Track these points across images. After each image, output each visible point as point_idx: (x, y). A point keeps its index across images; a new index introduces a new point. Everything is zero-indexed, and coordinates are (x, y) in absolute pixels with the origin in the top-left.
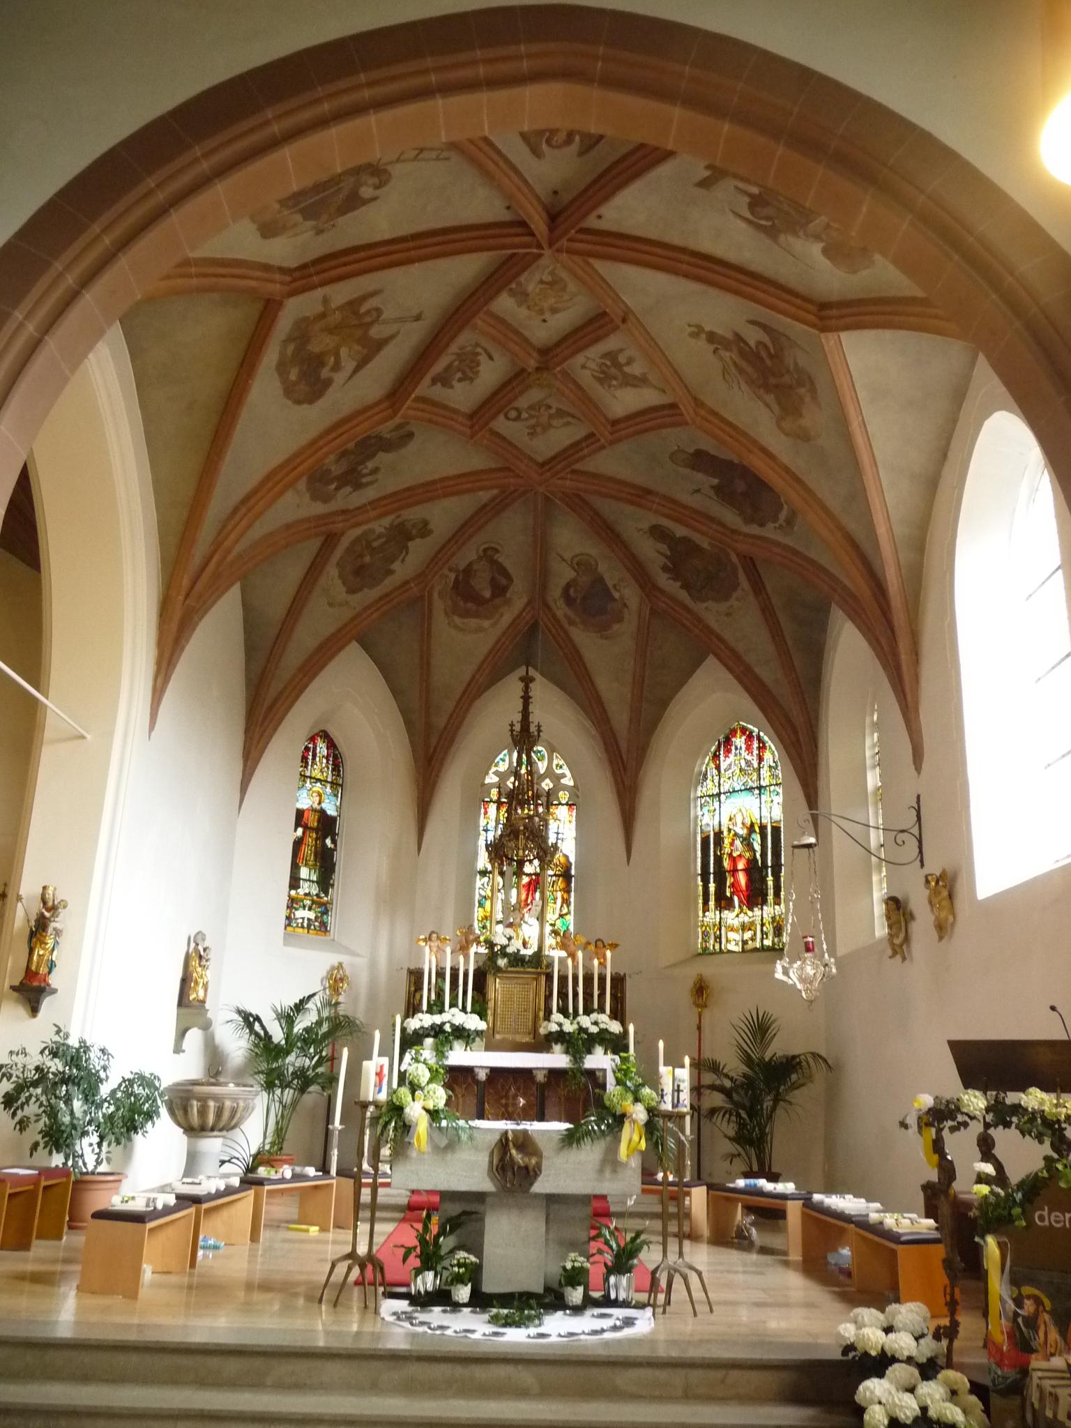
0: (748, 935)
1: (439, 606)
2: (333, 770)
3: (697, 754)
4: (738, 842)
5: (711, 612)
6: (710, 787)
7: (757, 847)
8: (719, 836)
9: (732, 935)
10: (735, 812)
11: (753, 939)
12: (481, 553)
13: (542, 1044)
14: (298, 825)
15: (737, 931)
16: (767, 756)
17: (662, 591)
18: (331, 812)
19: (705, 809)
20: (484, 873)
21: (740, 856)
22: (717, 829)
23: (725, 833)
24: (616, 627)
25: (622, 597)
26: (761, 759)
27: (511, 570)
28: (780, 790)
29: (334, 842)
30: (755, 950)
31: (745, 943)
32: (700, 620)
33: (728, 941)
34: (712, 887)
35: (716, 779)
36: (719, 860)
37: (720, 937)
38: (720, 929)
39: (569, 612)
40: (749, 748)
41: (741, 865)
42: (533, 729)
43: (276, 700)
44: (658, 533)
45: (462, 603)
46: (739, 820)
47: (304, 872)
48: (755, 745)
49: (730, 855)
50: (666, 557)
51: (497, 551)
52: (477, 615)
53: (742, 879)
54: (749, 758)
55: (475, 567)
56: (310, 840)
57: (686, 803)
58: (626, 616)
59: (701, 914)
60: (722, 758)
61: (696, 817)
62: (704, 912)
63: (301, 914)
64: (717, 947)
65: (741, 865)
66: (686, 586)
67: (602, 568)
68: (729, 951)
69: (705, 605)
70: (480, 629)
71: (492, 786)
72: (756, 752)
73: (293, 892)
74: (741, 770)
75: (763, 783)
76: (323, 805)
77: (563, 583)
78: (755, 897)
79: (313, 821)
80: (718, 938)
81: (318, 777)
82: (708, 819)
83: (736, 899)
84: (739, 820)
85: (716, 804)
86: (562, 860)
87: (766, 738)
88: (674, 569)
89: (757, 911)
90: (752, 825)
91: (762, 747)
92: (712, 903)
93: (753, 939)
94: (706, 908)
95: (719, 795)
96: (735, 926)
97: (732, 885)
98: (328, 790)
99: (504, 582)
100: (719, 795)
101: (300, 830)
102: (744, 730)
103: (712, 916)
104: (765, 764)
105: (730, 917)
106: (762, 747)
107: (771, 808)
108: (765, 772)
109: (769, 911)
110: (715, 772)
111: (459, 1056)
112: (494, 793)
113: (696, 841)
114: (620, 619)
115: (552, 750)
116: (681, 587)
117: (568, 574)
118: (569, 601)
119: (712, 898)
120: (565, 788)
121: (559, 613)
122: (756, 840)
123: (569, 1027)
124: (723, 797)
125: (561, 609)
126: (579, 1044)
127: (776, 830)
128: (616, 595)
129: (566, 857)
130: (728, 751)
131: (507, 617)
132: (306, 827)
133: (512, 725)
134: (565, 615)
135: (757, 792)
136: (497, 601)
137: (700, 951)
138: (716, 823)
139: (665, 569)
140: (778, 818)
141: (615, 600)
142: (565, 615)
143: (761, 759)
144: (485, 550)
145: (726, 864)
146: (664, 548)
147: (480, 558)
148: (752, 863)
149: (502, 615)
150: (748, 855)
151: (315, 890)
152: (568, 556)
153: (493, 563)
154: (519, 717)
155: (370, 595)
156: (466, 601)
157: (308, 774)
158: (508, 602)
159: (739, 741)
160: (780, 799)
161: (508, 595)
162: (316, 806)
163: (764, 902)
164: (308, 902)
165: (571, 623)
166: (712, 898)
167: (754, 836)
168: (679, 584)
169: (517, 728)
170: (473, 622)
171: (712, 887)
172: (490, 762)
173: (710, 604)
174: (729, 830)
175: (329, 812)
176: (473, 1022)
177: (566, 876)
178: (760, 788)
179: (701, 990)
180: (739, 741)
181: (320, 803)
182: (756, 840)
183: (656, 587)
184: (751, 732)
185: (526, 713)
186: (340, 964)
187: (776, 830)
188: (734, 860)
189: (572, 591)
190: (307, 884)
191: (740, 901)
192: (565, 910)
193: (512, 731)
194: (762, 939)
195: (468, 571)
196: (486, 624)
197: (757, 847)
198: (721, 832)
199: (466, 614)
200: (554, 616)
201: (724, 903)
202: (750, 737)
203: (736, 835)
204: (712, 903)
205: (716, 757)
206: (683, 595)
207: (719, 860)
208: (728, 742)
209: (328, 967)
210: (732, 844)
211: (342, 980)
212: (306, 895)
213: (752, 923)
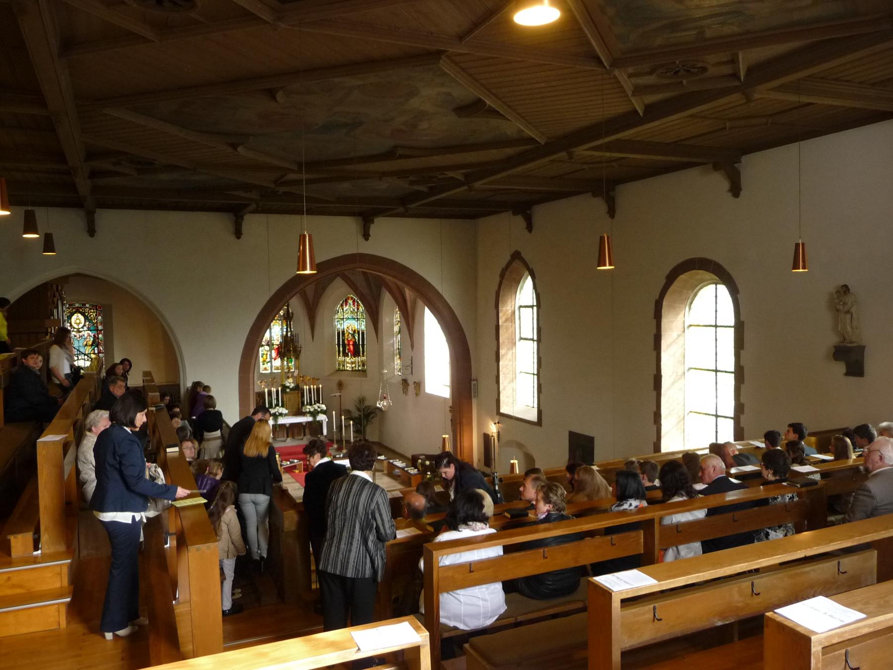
13: (303, 414)
53: (352, 347)
78: (356, 353)
91: (358, 305)
96: (350, 363)
105: (348, 359)
111: (281, 421)
123: (312, 410)
126: (314, 414)
148: (355, 343)
159: (350, 302)
176: (285, 411)
179: (340, 385)
180: (350, 302)
188: (349, 341)
201: (345, 355)
202: (354, 301)
205: (342, 305)
208: (346, 301)
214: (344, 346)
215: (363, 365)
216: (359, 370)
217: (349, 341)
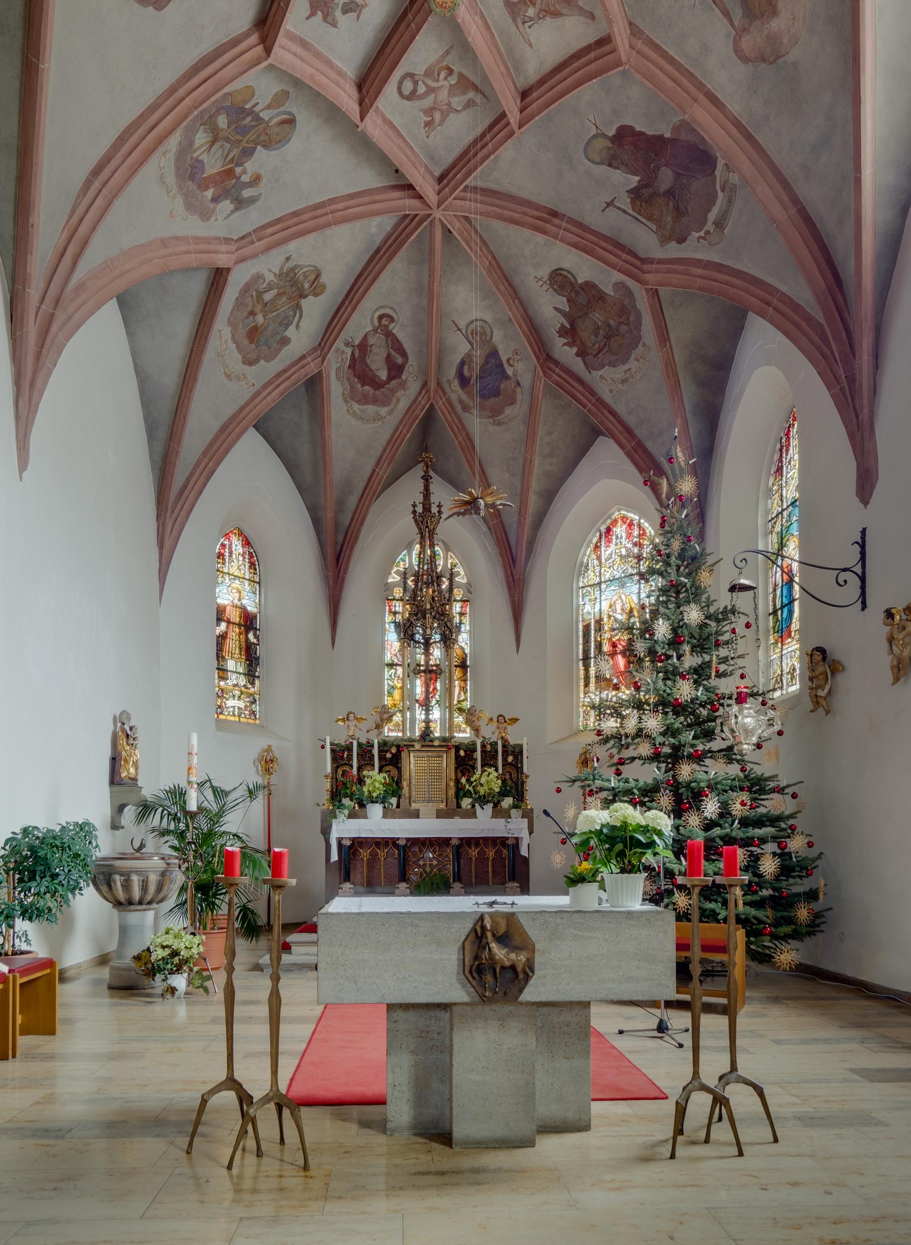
1: (336, 388)
2: (250, 568)
5: (606, 381)
6: (592, 577)
8: (599, 622)
12: (376, 323)
14: (219, 620)
17: (557, 363)
18: (252, 609)
19: (586, 599)
20: (391, 665)
22: (597, 617)
23: (605, 620)
24: (508, 411)
25: (515, 375)
27: (407, 345)
29: (256, 637)
32: (593, 393)
36: (599, 646)
39: (464, 397)
40: (629, 535)
42: (434, 510)
43: (185, 486)
44: (560, 280)
45: (359, 386)
46: (619, 607)
47: (231, 665)
50: (564, 314)
51: (392, 320)
52: (375, 401)
55: (371, 341)
56: (234, 633)
57: (568, 593)
58: (519, 396)
59: (582, 695)
60: (603, 549)
61: (578, 606)
62: (585, 694)
63: (231, 703)
66: (581, 354)
67: (498, 338)
69: (601, 372)
70: (378, 418)
71: (395, 585)
73: (222, 683)
76: (244, 602)
77: (457, 359)
79: (235, 616)
81: (236, 574)
82: (589, 609)
84: (619, 607)
85: (597, 593)
86: (459, 652)
87: (646, 525)
88: (570, 333)
95: (600, 584)
98: (247, 587)
99: (400, 360)
100: (600, 584)
101: (223, 626)
102: (624, 519)
112: (398, 592)
113: (578, 629)
114: (512, 402)
115: (447, 549)
116: (577, 354)
117: (464, 348)
118: (464, 381)
120: (460, 586)
121: (454, 398)
124: (603, 586)
125: (455, 391)
128: (510, 371)
129: (462, 648)
130: (610, 541)
131: (403, 400)
132: (229, 622)
133: (414, 506)
134: (461, 401)
136: (393, 383)
138: (597, 610)
139: (563, 332)
141: (508, 378)
142: (461, 401)
144: (381, 317)
146: (562, 302)
147: (375, 330)
149: (398, 401)
151: (242, 681)
152: (462, 324)
153: (389, 334)
154: (420, 498)
155: (268, 369)
156: (363, 385)
157: (226, 570)
158: (403, 385)
159: (620, 530)
161: (404, 377)
162: (236, 602)
164: (237, 693)
165: (465, 408)
168: (575, 350)
169: (419, 509)
170: (371, 409)
172: (392, 562)
173: (607, 371)
174: (609, 617)
175: (249, 608)
177: (463, 666)
181: (239, 600)
183: (549, 357)
184: (632, 521)
185: (427, 494)
186: (270, 747)
189: (466, 372)
190: (234, 676)
192: (462, 698)
193: (414, 512)
195: (363, 347)
196: (383, 411)
198: (601, 619)
199: (364, 400)
200: (449, 401)
206: (578, 366)
209: (259, 750)
211: (272, 761)
212: (235, 685)
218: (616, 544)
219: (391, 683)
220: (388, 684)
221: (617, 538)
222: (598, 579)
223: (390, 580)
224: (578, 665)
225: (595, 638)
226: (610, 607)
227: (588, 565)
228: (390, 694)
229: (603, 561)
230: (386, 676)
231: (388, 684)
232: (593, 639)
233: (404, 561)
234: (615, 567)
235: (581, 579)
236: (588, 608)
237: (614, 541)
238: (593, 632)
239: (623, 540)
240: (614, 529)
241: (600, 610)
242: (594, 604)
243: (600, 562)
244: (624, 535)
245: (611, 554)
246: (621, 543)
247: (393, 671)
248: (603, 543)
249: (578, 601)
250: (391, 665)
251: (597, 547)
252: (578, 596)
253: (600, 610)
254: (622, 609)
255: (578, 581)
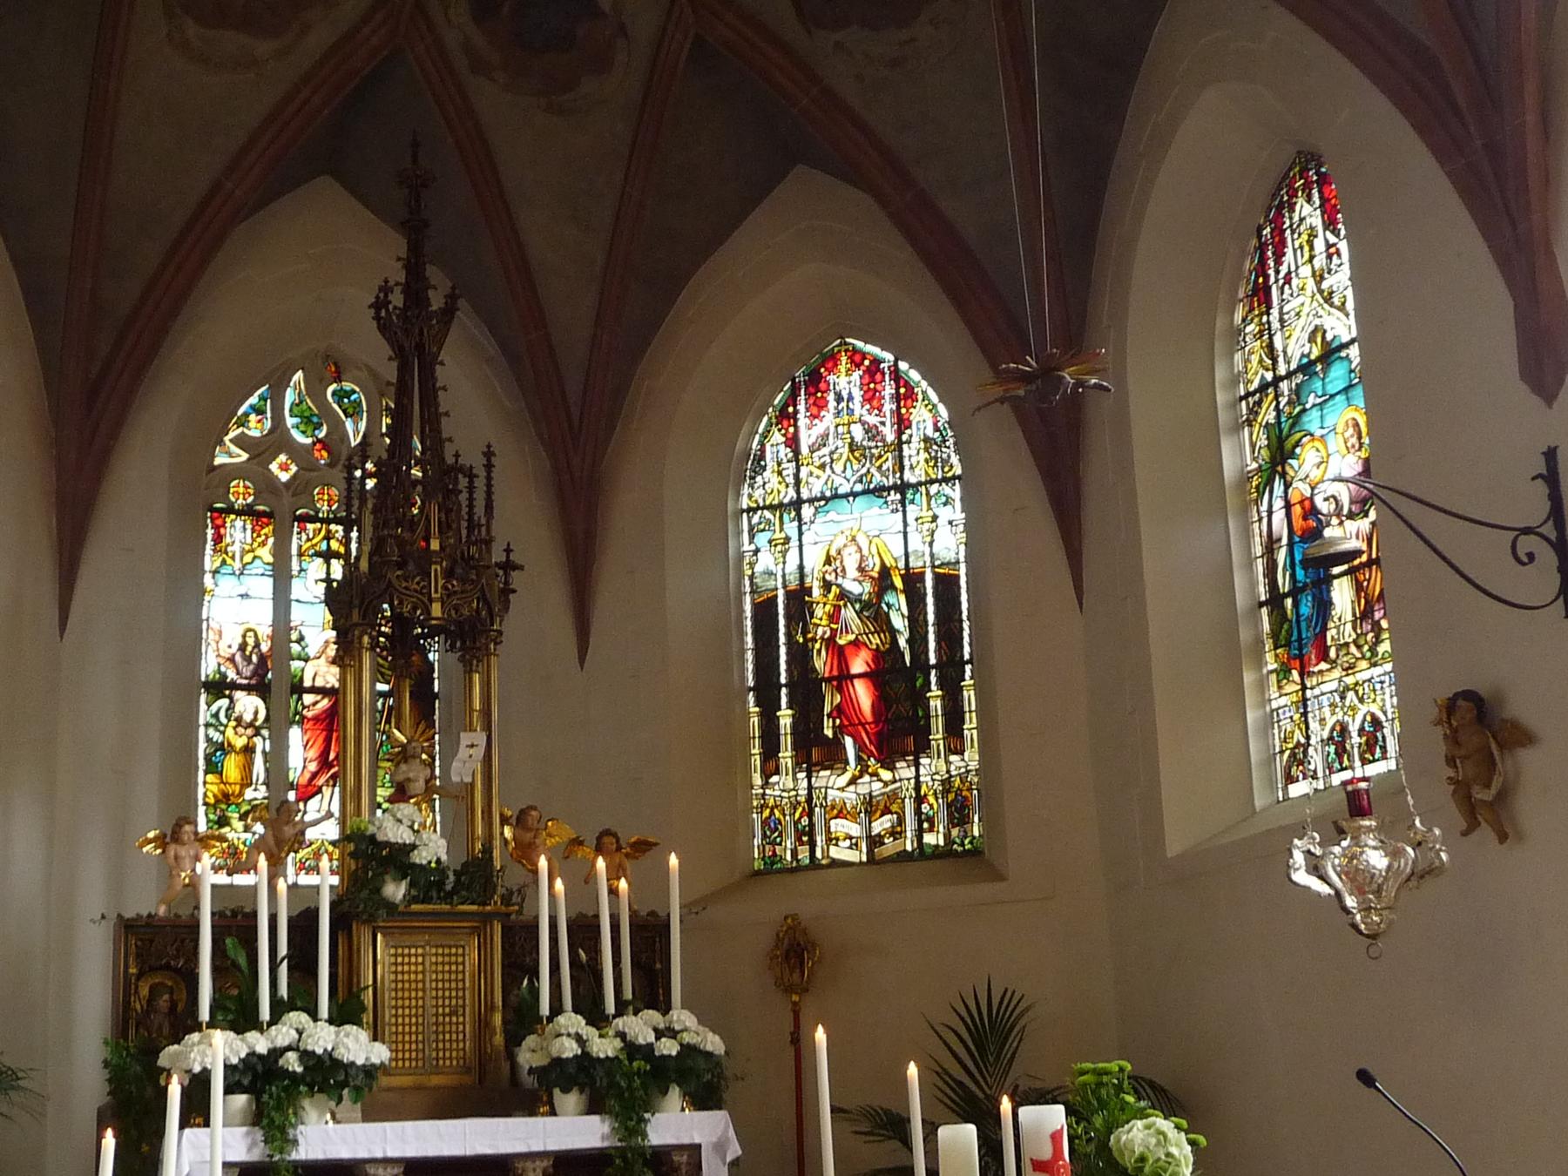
0: (881, 825)
3: (745, 407)
4: (849, 613)
7: (899, 622)
8: (799, 598)
9: (840, 826)
10: (840, 542)
11: (896, 833)
15: (852, 816)
16: (921, 417)
19: (762, 539)
21: (856, 644)
22: (793, 584)
26: (902, 424)
28: (955, 492)
30: (903, 856)
31: (874, 841)
33: (831, 840)
34: (785, 717)
35: (790, 469)
36: (801, 656)
37: (811, 833)
38: (810, 814)
40: (871, 397)
41: (858, 665)
46: (851, 563)
48: (888, 389)
49: (830, 642)
54: (873, 420)
57: (717, 525)
59: (757, 779)
60: (803, 422)
61: (741, 556)
64: (804, 853)
65: (858, 665)
68: (835, 863)
72: (888, 406)
74: (853, 447)
75: (909, 477)
78: (897, 735)
80: (806, 835)
82: (769, 562)
83: (849, 742)
84: (851, 563)
85: (791, 529)
87: (915, 375)
89: (905, 771)
90: (885, 572)
92: (786, 756)
93: (896, 833)
94: (770, 767)
95: (797, 504)
96: (848, 808)
97: (839, 711)
100: (797, 504)
102: (857, 358)
103: (788, 783)
104: (915, 434)
105: (835, 785)
106: (905, 395)
107: (940, 535)
108: (914, 453)
109: (932, 767)
110: (785, 452)
119: (786, 741)
122: (898, 609)
124: (807, 511)
127: (947, 584)
130: (818, 406)
135: (895, 496)
137: (758, 865)
140: (951, 557)
143: (902, 424)
145: (821, 663)
150: (875, 640)
159: (846, 381)
160: (959, 516)
163: (923, 747)
166: (786, 741)
167: (890, 597)
171: (785, 717)
174: (827, 586)
178: (902, 488)
182: (898, 609)
184: (876, 362)
187: (947, 584)
191: (860, 747)
194: (920, 832)
197: (899, 622)
201: (817, 752)
203: (844, 595)
204: (786, 756)
207: (801, 656)
208: (815, 382)
210: (834, 617)
213: (893, 797)
214: (807, 691)
215: (958, 813)
216: (922, 853)
217: (840, 655)
218: (838, 414)
219: (216, 736)
220: (209, 740)
221: (839, 399)
222: (792, 493)
223: (218, 461)
224: (745, 702)
225: (789, 635)
226: (828, 561)
227: (762, 457)
228: (213, 767)
229: (805, 450)
230: (204, 715)
231: (209, 740)
232: (782, 639)
233: (259, 411)
234: (838, 467)
235: (746, 490)
236: (766, 561)
237: (832, 404)
238: (782, 622)
239: (856, 405)
240: (831, 378)
241: (801, 567)
242: (784, 553)
243: (797, 452)
244: (858, 394)
245: (825, 436)
246: (851, 412)
247: (224, 702)
248: (801, 407)
249: (740, 545)
250: (219, 687)
251: (786, 416)
252: (739, 533)
253: (801, 567)
254: (861, 569)
255: (738, 495)
